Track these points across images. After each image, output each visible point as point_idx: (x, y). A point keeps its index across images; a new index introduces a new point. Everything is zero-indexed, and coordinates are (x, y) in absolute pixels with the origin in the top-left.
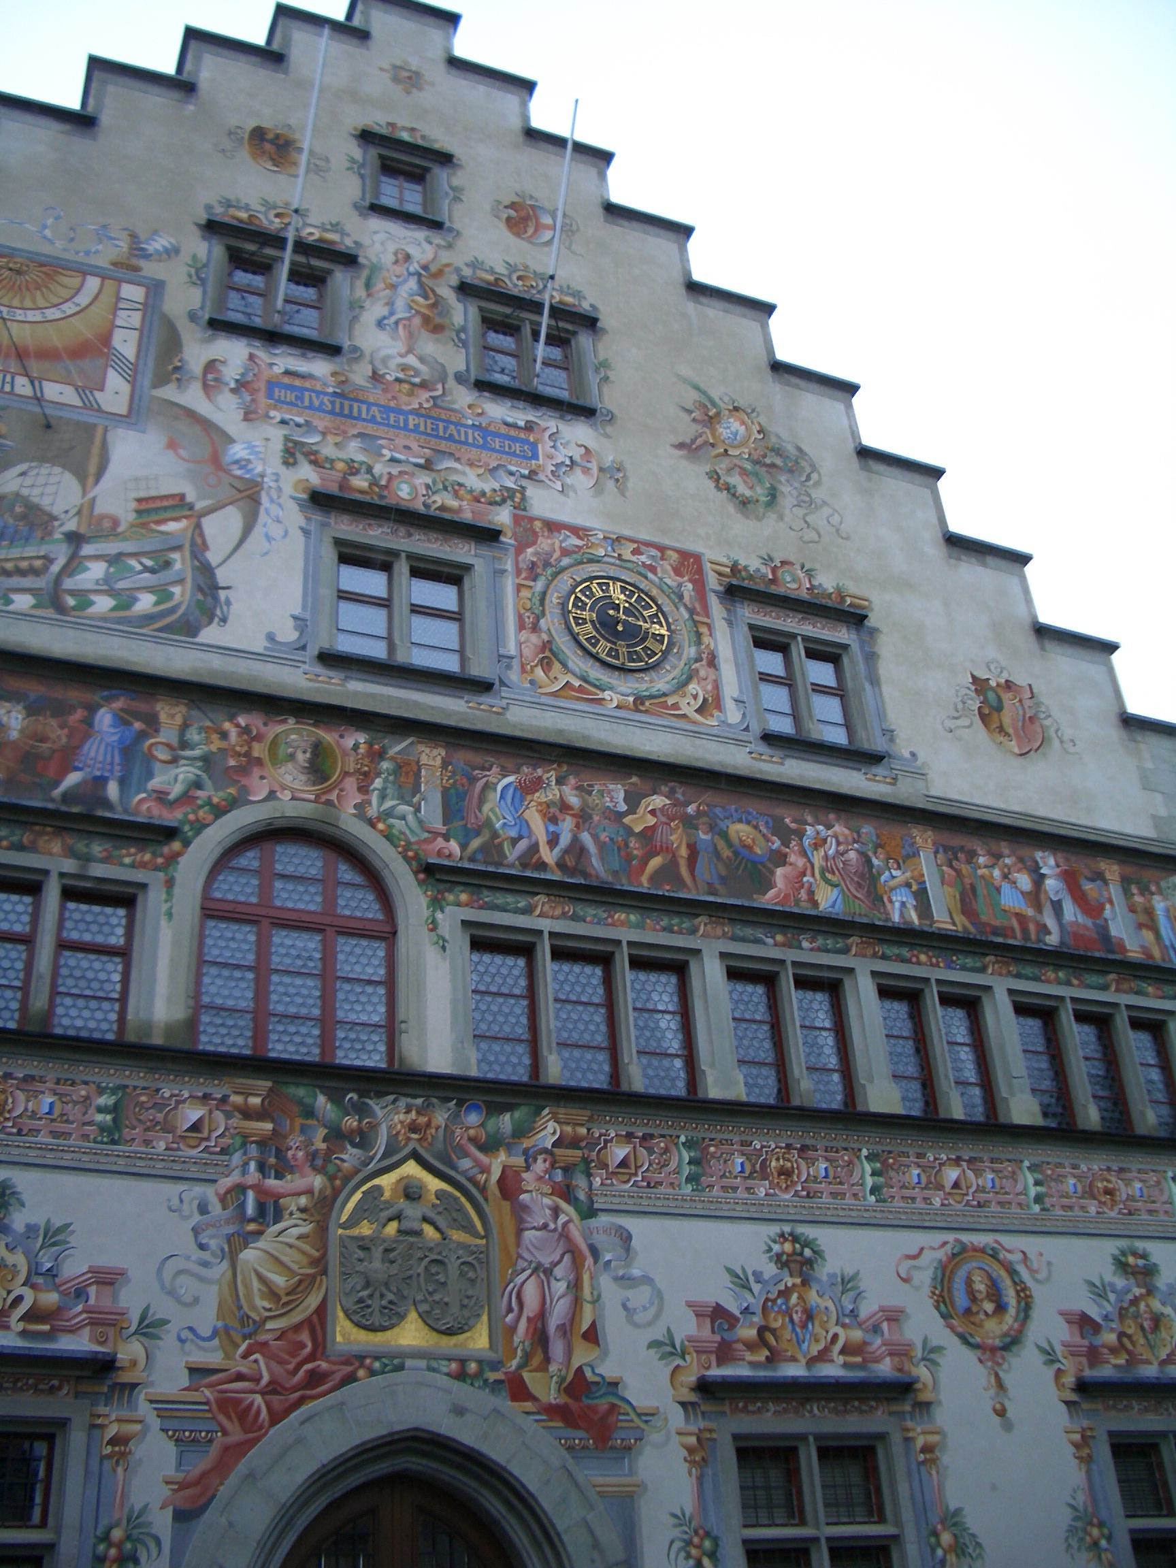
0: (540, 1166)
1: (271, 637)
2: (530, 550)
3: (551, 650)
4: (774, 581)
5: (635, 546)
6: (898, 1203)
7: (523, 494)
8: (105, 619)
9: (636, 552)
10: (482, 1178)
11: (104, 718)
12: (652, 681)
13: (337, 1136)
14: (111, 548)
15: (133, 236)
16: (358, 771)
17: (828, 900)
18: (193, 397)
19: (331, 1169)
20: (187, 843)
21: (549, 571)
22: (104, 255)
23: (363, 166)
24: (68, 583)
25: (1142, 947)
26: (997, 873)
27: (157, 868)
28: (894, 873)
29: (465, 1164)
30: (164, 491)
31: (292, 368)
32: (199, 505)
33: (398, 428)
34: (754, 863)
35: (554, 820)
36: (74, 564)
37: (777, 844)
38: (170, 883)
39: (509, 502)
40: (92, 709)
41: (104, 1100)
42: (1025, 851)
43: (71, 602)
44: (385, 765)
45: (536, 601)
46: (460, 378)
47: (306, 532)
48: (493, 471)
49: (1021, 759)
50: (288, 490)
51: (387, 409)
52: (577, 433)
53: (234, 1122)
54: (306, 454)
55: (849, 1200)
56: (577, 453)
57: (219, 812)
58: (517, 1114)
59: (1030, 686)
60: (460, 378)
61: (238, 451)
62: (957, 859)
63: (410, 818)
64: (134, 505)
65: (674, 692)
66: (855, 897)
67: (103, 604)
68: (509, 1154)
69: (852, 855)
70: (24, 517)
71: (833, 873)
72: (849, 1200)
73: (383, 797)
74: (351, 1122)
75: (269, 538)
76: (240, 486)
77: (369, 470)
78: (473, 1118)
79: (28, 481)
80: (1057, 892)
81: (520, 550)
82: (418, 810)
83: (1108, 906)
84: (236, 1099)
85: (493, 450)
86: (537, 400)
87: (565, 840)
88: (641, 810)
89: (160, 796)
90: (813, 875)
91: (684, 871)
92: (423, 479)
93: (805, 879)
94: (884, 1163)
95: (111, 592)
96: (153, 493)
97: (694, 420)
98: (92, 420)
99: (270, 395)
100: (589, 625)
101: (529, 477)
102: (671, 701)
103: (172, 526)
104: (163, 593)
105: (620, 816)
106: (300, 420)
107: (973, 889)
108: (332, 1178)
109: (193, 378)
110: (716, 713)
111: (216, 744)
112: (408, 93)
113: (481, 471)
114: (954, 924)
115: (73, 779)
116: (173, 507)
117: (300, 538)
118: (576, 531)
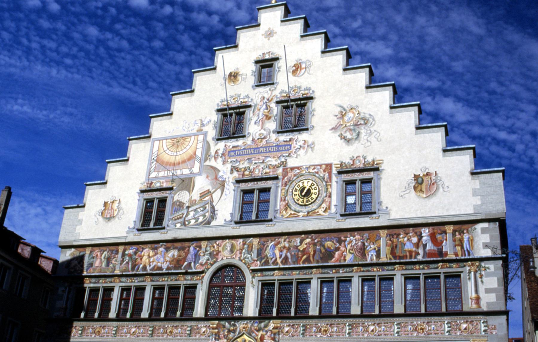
0: (269, 333)
1: (225, 220)
2: (286, 178)
3: (288, 206)
4: (353, 165)
5: (313, 167)
6: (355, 336)
7: (286, 162)
8: (193, 225)
9: (314, 169)
10: (256, 337)
11: (192, 248)
12: (312, 206)
13: (229, 331)
14: (194, 208)
15: (201, 121)
16: (240, 249)
17: (349, 258)
18: (212, 163)
19: (228, 338)
20: (206, 273)
21: (290, 182)
22: (196, 128)
23: (255, 72)
24: (187, 219)
25: (454, 253)
26: (406, 239)
27: (200, 280)
28: (371, 246)
29: (254, 335)
30: (205, 190)
31: (234, 145)
32: (212, 191)
33: (257, 153)
34: (330, 252)
35: (281, 251)
36: (188, 214)
37: (338, 245)
38: (202, 282)
39: (282, 166)
40: (189, 247)
41: (189, 329)
42: (417, 230)
43: (187, 223)
44: (246, 246)
45: (286, 192)
46: (274, 132)
47: (234, 190)
48: (279, 158)
49: (426, 199)
50: (231, 180)
51: (255, 149)
52: (303, 136)
53: (211, 330)
54: (235, 169)
55: (341, 336)
56: (301, 143)
57: (212, 265)
58: (265, 323)
59: (436, 172)
60: (274, 132)
61: (221, 174)
62: (393, 237)
63: (250, 258)
64: (199, 195)
65: (317, 208)
66: (358, 256)
67: (193, 222)
68: (263, 332)
69: (360, 244)
70: (179, 205)
71: (352, 250)
72: (341, 336)
73: (244, 254)
74: (232, 328)
75: (226, 195)
76: (220, 183)
77: (249, 169)
78: (256, 325)
79: (180, 196)
80: (426, 241)
81: (283, 179)
82: (251, 255)
83: (445, 242)
84: (211, 326)
85: (280, 151)
86: (292, 131)
87: (283, 256)
88: (303, 244)
89: (201, 264)
90: (346, 252)
91: (311, 258)
92: (262, 166)
93: (344, 254)
94: (353, 327)
95: (195, 218)
96: (203, 191)
97: (338, 118)
98: (191, 176)
99: (228, 155)
100: (298, 196)
101: (288, 156)
102: (316, 211)
103: (207, 198)
104: (204, 216)
105: (298, 246)
106: (235, 160)
107: (396, 246)
108: (228, 340)
109: (212, 157)
110: (329, 211)
111: (212, 249)
112: (269, 39)
113: (276, 158)
114: (387, 258)
115: (186, 263)
116: (207, 194)
117: (233, 192)
118: (298, 168)
